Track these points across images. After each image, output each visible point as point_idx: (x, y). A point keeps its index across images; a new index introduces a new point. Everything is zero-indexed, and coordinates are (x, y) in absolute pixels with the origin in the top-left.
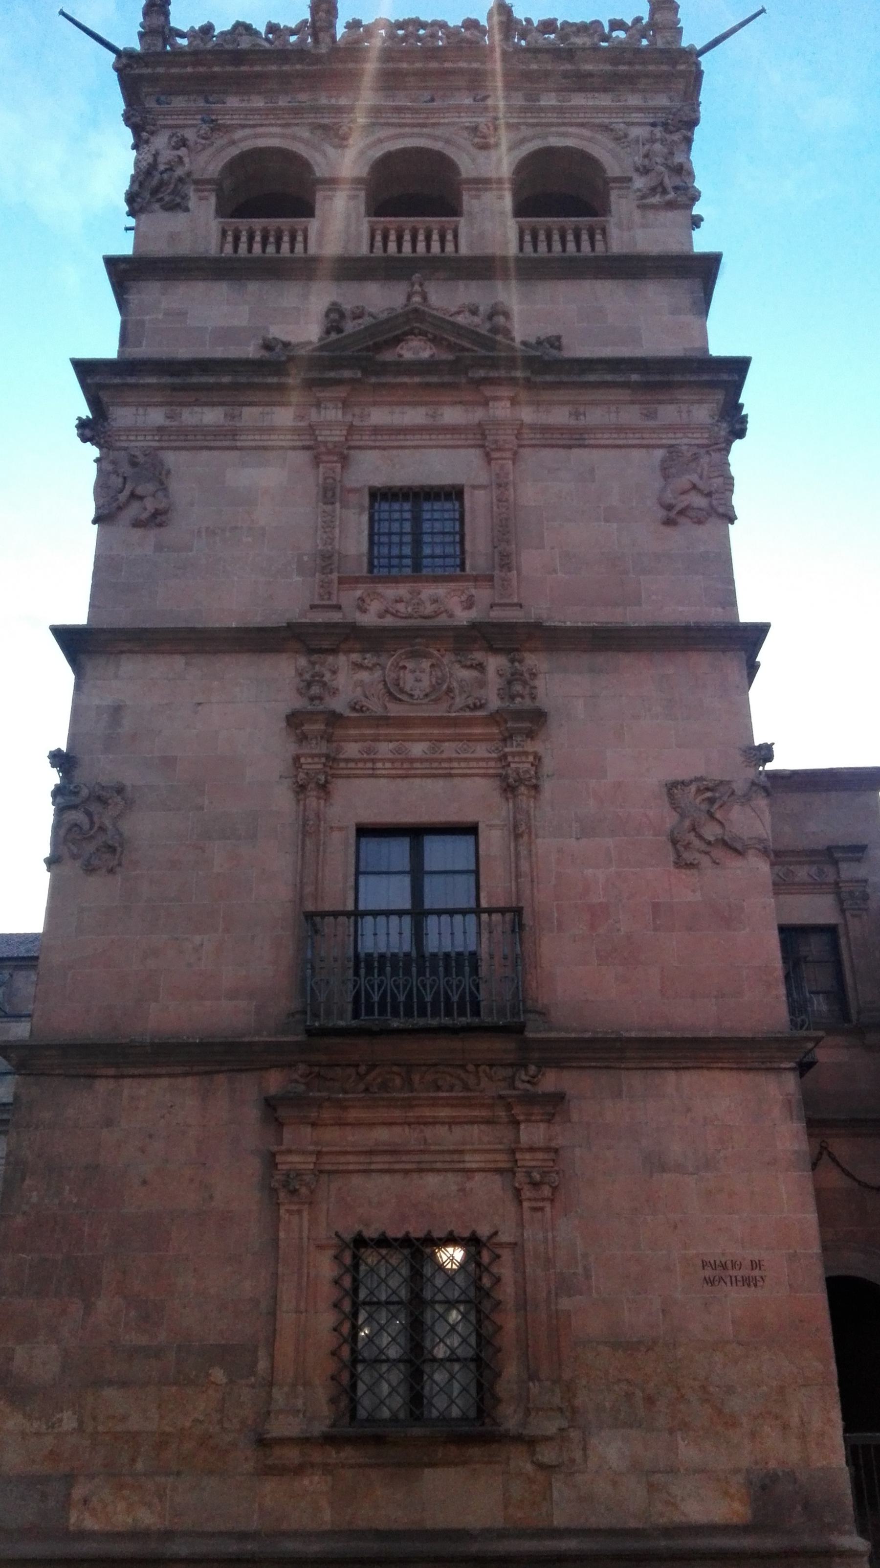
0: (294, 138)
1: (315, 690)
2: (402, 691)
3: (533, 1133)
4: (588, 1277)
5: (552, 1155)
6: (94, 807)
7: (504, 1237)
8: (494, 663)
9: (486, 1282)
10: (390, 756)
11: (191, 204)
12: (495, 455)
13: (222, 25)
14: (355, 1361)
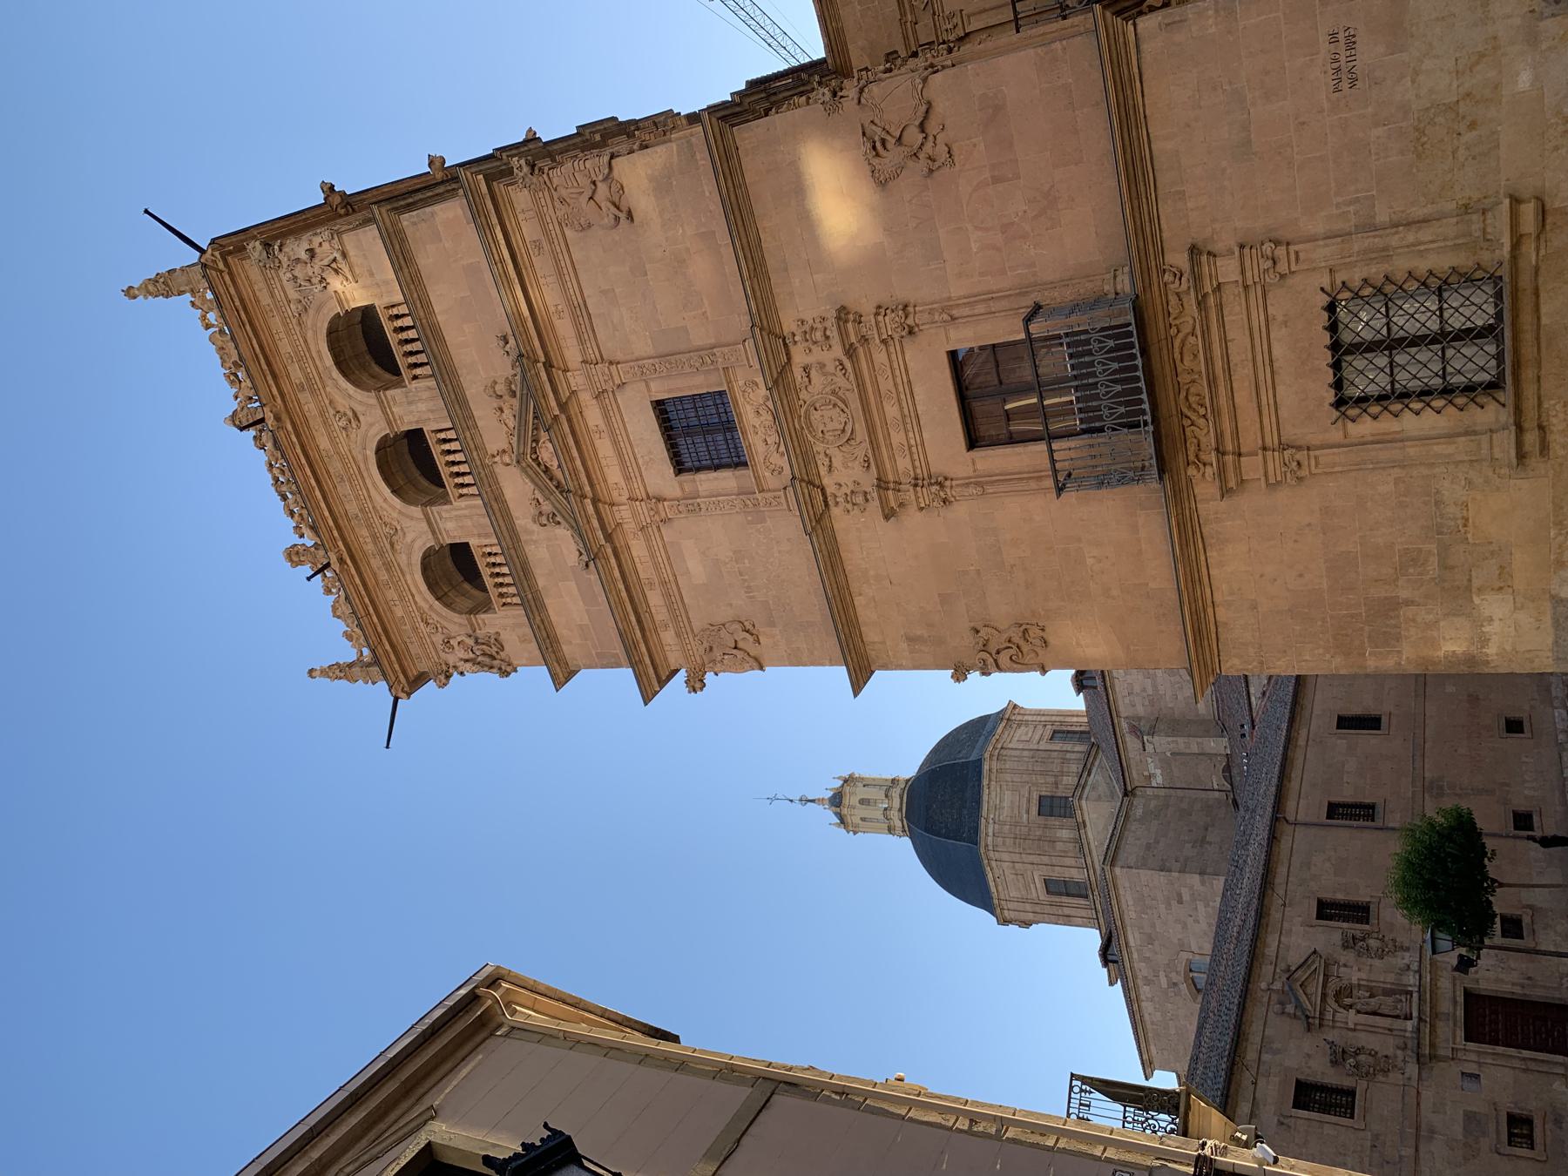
0: (409, 564)
1: (860, 499)
2: (843, 431)
3: (1228, 270)
4: (1357, 200)
5: (1246, 250)
6: (993, 648)
8: (799, 357)
9: (1367, 291)
10: (902, 433)
11: (492, 631)
12: (618, 382)
13: (341, 626)
14: (1447, 391)
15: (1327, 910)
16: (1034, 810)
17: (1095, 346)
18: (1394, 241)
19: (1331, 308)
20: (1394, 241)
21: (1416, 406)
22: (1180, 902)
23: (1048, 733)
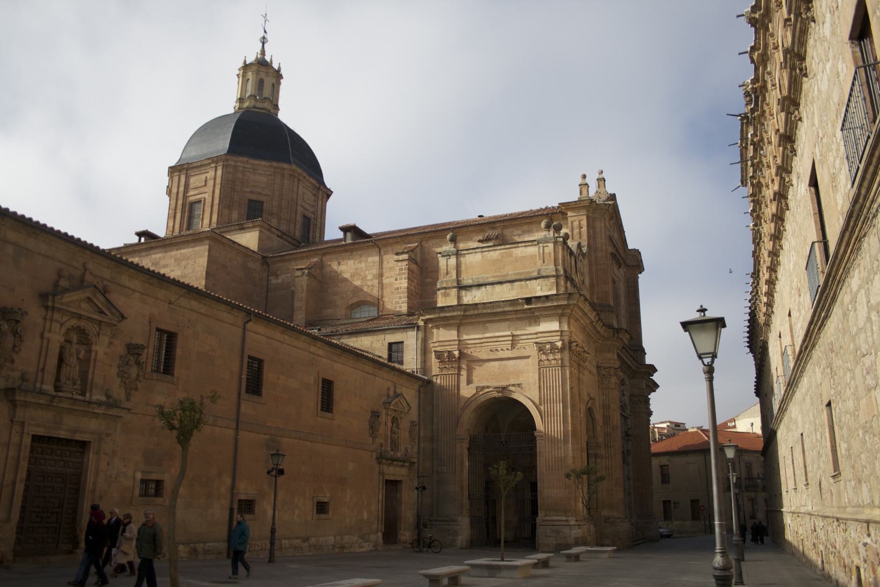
15: (169, 339)
16: (253, 197)
23: (309, 215)
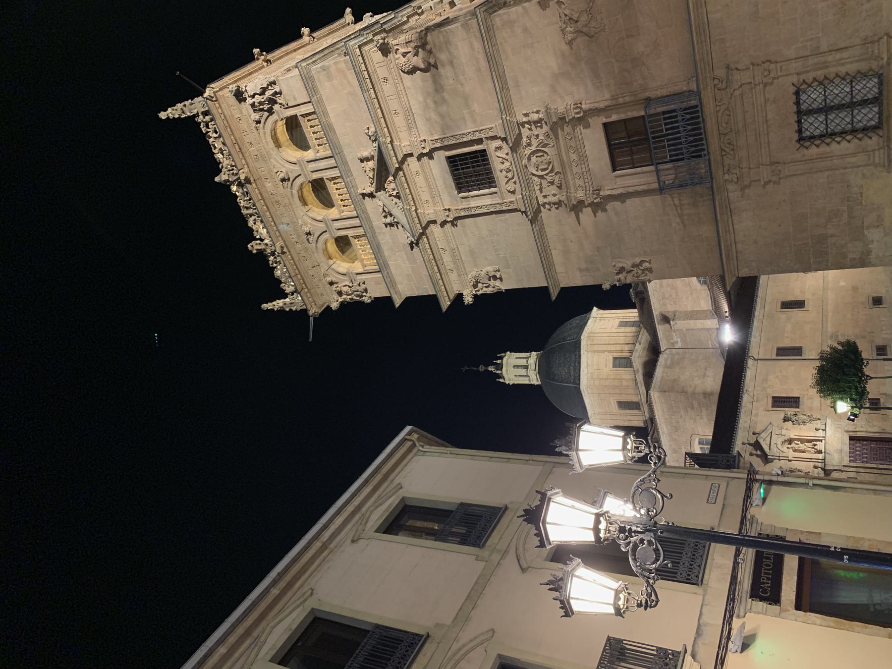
4: (812, 39)
7: (795, 79)
14: (854, 131)
17: (680, 118)
18: (830, 58)
19: (797, 93)
20: (830, 58)
21: (838, 139)
22: (692, 408)
